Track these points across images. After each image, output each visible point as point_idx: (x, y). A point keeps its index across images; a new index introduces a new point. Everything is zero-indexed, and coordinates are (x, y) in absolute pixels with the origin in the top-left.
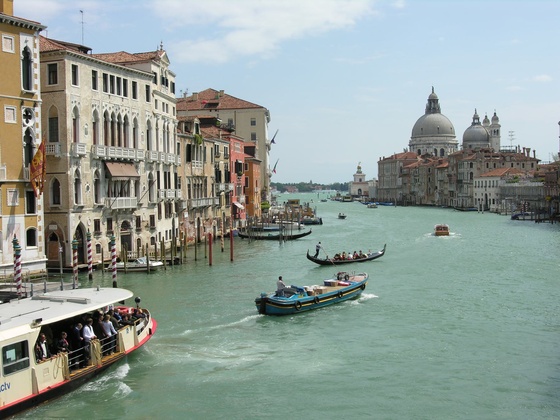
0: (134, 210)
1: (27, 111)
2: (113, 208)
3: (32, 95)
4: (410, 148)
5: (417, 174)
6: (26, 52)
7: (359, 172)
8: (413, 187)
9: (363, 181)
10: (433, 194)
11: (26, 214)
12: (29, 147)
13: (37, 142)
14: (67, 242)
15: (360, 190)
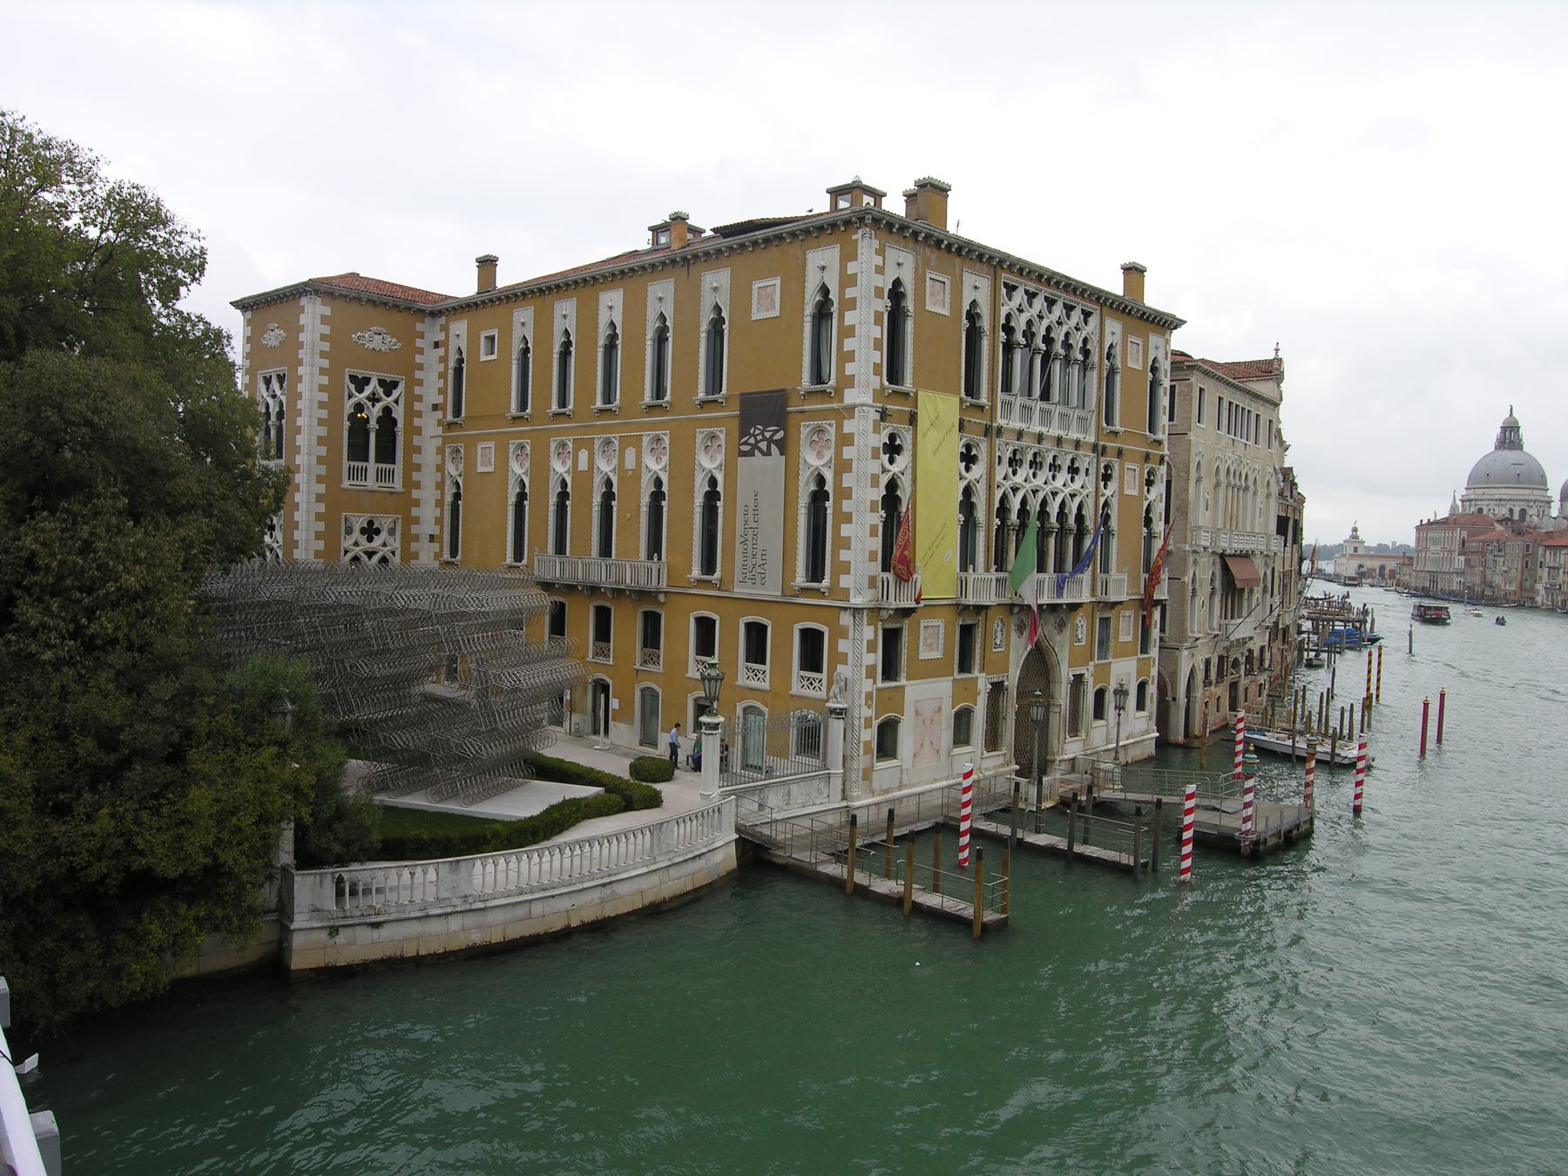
0: (1251, 638)
1: (1149, 473)
2: (1232, 638)
3: (1159, 443)
4: (1463, 506)
5: (1500, 554)
6: (1154, 370)
7: (1355, 537)
8: (1488, 572)
9: (1360, 551)
10: (1532, 589)
11: (1140, 656)
12: (1150, 537)
13: (1159, 526)
14: (1174, 699)
15: (1361, 566)
